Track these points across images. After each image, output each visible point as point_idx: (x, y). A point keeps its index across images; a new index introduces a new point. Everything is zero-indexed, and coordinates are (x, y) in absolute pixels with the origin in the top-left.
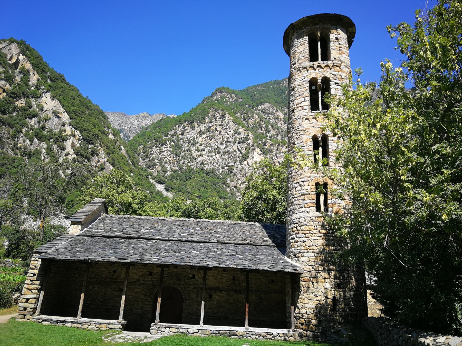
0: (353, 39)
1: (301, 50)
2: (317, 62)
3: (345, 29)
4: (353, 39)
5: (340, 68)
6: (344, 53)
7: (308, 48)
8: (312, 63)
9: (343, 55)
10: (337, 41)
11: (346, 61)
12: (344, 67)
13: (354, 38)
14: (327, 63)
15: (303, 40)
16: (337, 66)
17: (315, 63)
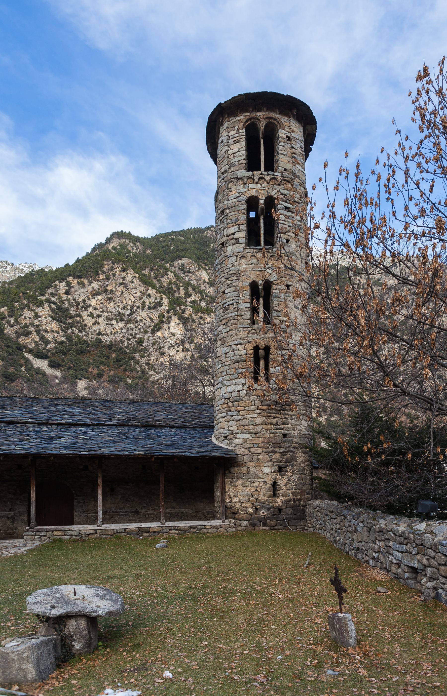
0: (311, 147)
1: (234, 151)
2: (260, 172)
4: (311, 147)
5: (292, 186)
6: (299, 164)
7: (244, 148)
8: (250, 173)
9: (297, 166)
10: (289, 142)
11: (301, 176)
12: (297, 184)
13: (312, 145)
14: (274, 175)
15: (237, 135)
16: (289, 182)
17: (256, 173)
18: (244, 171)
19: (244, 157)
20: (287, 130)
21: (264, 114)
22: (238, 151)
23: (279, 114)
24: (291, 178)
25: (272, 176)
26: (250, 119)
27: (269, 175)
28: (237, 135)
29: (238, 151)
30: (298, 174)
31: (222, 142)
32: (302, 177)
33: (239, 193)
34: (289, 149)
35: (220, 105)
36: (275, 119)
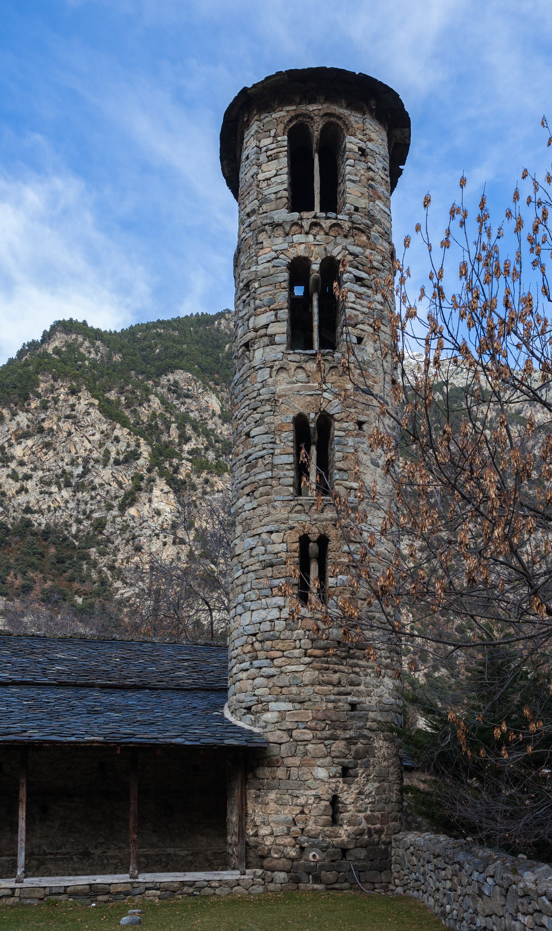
0: (401, 167)
1: (268, 175)
2: (312, 214)
3: (385, 127)
4: (401, 167)
5: (369, 238)
6: (380, 198)
7: (286, 170)
8: (296, 215)
9: (377, 202)
10: (363, 158)
11: (383, 220)
12: (377, 235)
13: (403, 164)
14: (336, 218)
15: (274, 146)
16: (362, 231)
17: (305, 215)
18: (284, 211)
19: (286, 186)
20: (360, 137)
21: (320, 107)
22: (276, 175)
23: (347, 108)
24: (366, 225)
25: (334, 221)
26: (296, 117)
27: (328, 218)
28: (274, 146)
29: (276, 175)
30: (379, 217)
31: (247, 158)
32: (386, 222)
33: (276, 251)
34: (362, 172)
35: (245, 91)
36: (339, 118)
